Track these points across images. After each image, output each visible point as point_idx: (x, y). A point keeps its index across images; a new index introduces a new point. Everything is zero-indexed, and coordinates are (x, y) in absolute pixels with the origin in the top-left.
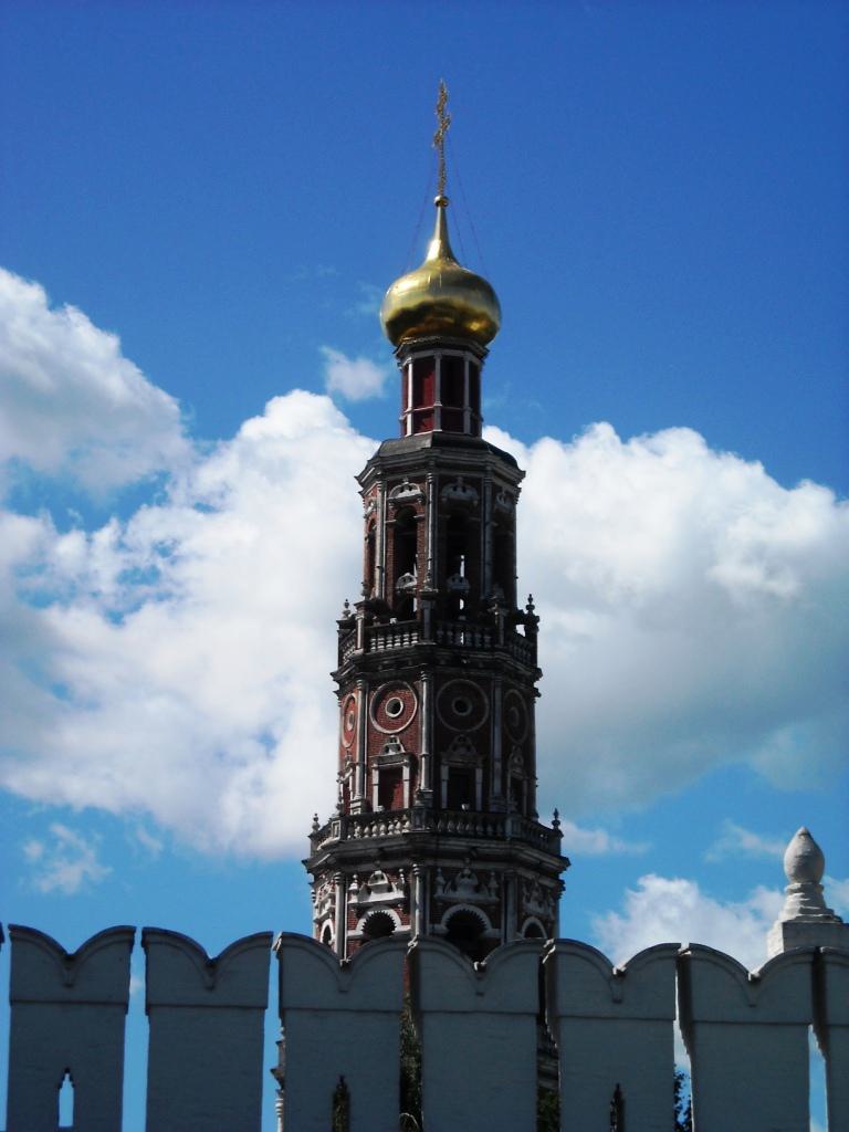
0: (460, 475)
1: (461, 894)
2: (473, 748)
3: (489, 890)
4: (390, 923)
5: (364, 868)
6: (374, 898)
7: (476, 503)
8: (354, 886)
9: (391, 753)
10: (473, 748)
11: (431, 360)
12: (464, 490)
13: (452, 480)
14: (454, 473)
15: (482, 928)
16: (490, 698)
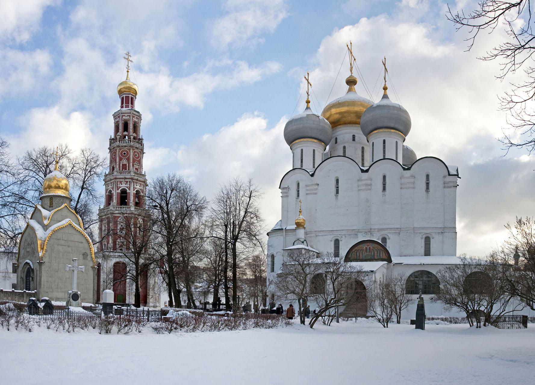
6: (122, 185)
8: (119, 183)
9: (124, 161)
11: (129, 96)
13: (135, 117)
14: (135, 116)
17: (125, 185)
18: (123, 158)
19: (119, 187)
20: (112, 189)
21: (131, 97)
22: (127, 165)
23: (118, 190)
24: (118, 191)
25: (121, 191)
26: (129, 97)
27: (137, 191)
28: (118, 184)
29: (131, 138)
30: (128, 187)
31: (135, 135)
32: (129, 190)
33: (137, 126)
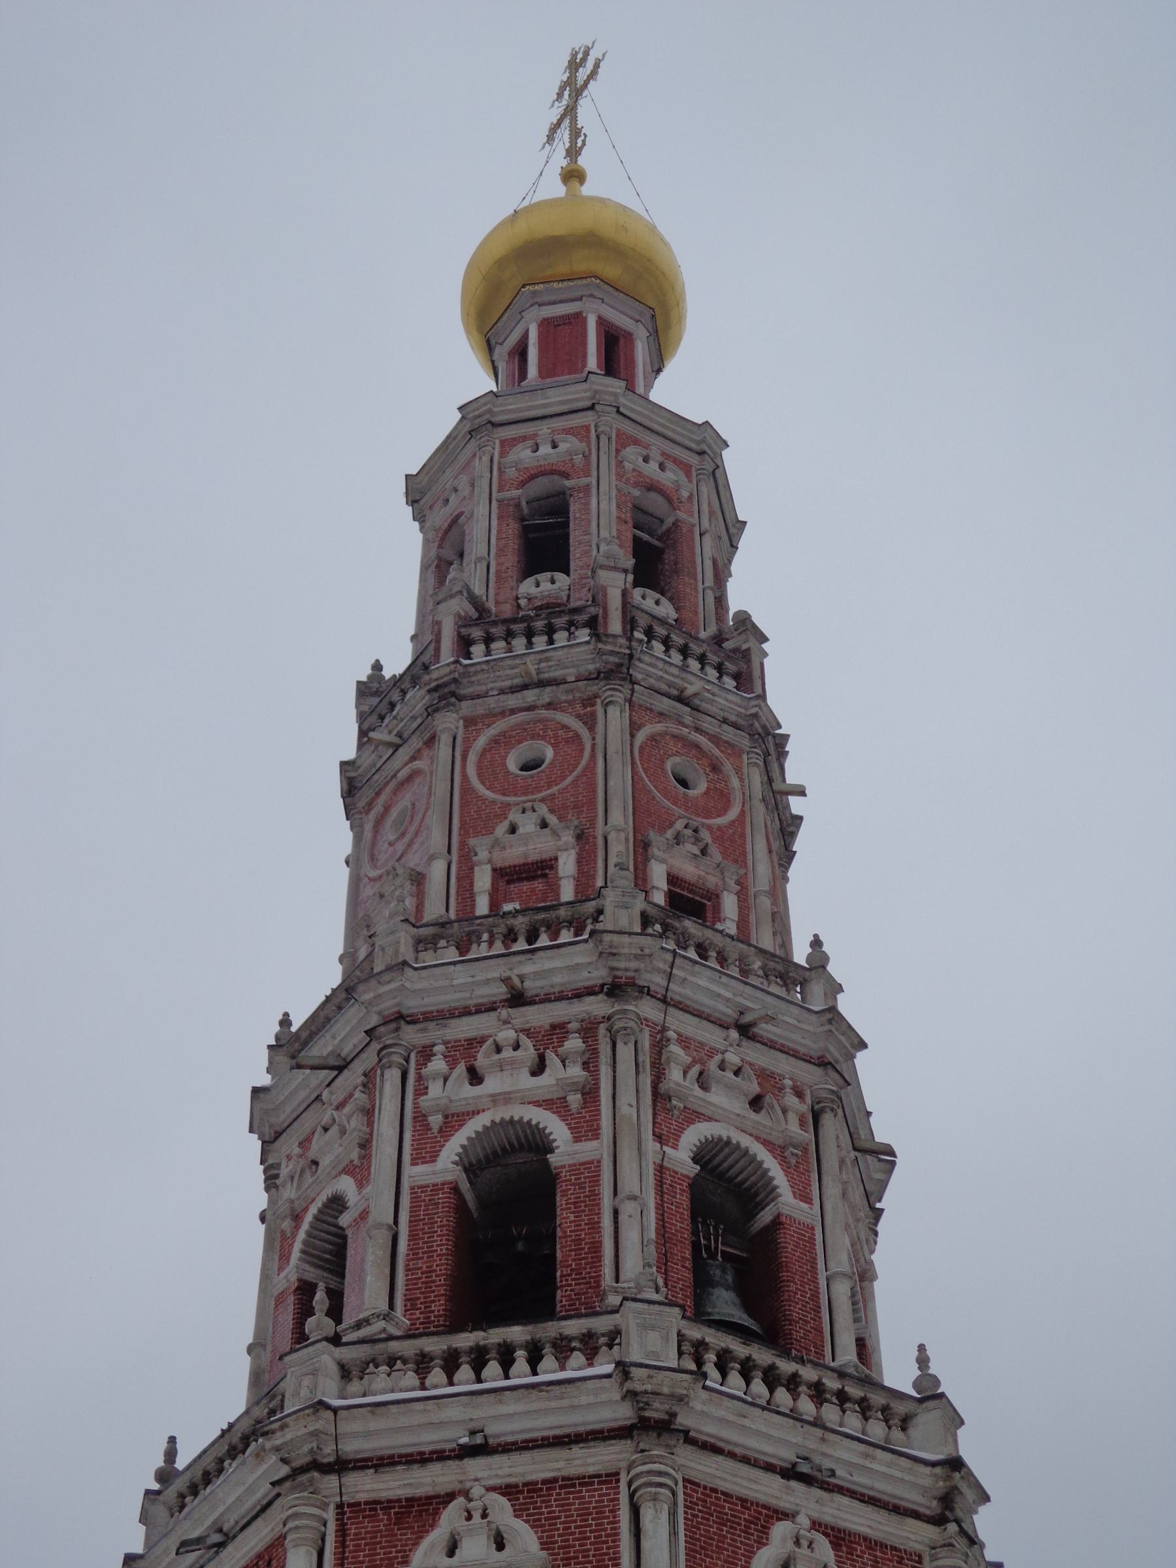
1: (717, 1098)
2: (714, 850)
3: (785, 1111)
6: (492, 1084)
8: (438, 1064)
10: (714, 850)
11: (577, 320)
12: (662, 467)
15: (771, 1192)
16: (741, 780)
17: (526, 1082)
18: (507, 807)
19: (436, 1120)
21: (601, 322)
22: (567, 865)
23: (427, 1153)
24: (420, 1169)
26: (584, 321)
27: (706, 1155)
28: (422, 1091)
29: (604, 590)
31: (666, 610)
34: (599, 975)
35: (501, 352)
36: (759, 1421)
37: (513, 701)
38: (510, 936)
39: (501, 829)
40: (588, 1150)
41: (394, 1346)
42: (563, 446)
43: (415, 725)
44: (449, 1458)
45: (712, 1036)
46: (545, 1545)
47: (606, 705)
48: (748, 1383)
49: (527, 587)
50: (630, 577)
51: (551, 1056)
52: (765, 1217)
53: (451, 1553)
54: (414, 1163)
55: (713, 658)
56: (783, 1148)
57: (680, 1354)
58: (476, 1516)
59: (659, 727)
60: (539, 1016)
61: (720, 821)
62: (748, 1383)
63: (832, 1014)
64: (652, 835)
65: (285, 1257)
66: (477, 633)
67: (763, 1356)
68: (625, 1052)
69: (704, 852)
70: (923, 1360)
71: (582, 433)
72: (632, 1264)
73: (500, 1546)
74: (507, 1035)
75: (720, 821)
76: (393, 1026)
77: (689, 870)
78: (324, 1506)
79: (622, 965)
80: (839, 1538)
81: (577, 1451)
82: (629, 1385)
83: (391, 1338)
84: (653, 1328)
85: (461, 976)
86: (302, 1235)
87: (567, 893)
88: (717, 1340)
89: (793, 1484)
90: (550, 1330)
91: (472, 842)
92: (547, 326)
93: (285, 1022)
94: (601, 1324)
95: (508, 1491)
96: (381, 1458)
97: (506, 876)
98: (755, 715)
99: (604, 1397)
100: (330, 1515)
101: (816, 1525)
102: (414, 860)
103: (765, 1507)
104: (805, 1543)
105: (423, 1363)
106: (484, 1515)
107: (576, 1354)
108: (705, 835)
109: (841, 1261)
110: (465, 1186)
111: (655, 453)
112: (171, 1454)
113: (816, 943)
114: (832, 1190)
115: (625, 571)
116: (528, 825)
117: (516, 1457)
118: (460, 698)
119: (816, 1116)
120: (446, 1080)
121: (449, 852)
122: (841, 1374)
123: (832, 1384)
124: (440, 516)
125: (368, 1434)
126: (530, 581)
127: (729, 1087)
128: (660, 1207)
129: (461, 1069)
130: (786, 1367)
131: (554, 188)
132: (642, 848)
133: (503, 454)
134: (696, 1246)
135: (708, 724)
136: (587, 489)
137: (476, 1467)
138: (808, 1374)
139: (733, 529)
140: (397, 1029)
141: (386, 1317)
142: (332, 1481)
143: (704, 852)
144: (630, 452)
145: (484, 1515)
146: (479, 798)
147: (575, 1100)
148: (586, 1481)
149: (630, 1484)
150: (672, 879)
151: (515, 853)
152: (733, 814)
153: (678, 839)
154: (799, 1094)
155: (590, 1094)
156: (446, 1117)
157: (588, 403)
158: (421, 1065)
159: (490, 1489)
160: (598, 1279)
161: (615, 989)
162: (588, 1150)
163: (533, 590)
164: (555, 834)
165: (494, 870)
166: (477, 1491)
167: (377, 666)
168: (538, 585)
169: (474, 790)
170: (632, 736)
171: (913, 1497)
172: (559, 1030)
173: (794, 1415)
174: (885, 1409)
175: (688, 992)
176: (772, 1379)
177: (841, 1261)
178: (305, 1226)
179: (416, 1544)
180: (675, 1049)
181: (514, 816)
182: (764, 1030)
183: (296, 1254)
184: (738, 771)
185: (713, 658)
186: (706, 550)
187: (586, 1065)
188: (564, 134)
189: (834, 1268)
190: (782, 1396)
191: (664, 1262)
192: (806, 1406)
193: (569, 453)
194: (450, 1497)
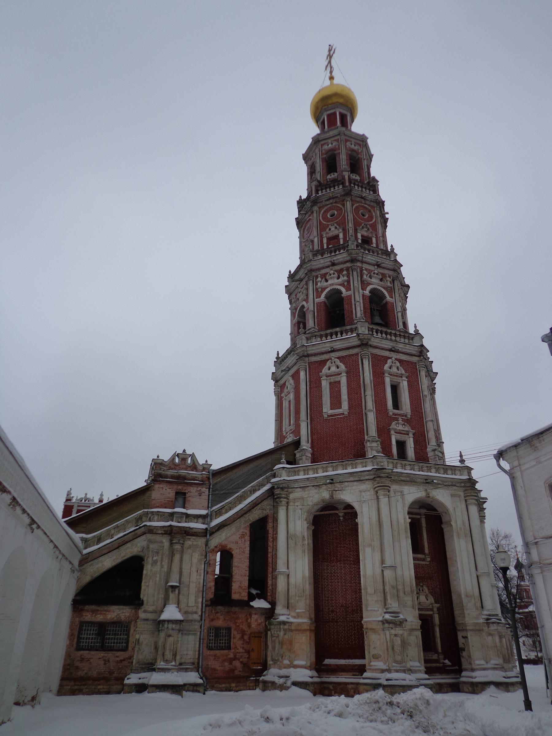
0: (353, 141)
1: (373, 280)
3: (387, 281)
4: (340, 292)
5: (323, 271)
6: (330, 282)
7: (360, 151)
8: (319, 279)
11: (335, 113)
12: (355, 145)
15: (385, 297)
16: (375, 213)
17: (336, 281)
18: (328, 225)
19: (320, 290)
20: (304, 303)
21: (340, 113)
22: (341, 236)
23: (319, 296)
25: (327, 297)
27: (371, 291)
28: (316, 284)
30: (346, 283)
31: (358, 178)
32: (348, 289)
33: (359, 158)
34: (349, 258)
35: (320, 123)
36: (384, 342)
37: (328, 203)
38: (331, 252)
39: (328, 230)
40: (349, 293)
41: (315, 334)
42: (334, 144)
43: (309, 209)
44: (327, 353)
45: (372, 268)
46: (346, 367)
47: (346, 201)
48: (382, 335)
49: (329, 177)
50: (349, 173)
51: (341, 275)
52: (384, 302)
53: (329, 370)
54: (316, 298)
55: (368, 188)
56: (387, 288)
57: (368, 330)
58: (333, 363)
59: (358, 204)
60: (337, 268)
61: (371, 222)
62: (382, 335)
63: (396, 260)
64: (357, 228)
65: (295, 317)
66: (319, 188)
67: (384, 329)
68: (355, 273)
69: (368, 229)
70: (415, 327)
71: (337, 140)
72: (359, 314)
73: (338, 368)
74: (332, 272)
75: (371, 222)
76: (310, 272)
77: (365, 234)
78: (306, 363)
79: (353, 256)
80: (400, 361)
81: (351, 350)
82: (359, 338)
83: (316, 332)
84: (363, 327)
85: (322, 261)
86: (297, 313)
87: (342, 242)
88: (375, 327)
89: (391, 352)
90: (344, 328)
91: (322, 233)
92: (329, 116)
93: (290, 272)
94: (353, 326)
95: (339, 358)
96: (315, 354)
97: (329, 239)
98: (377, 199)
99: (355, 340)
100: (307, 364)
101: (396, 359)
102: (311, 238)
103: (386, 357)
104: (394, 363)
105: (321, 336)
106: (335, 363)
107: (349, 332)
108: (368, 226)
109: (399, 309)
110: (326, 302)
111: (353, 143)
112: (278, 354)
113: (392, 246)
114: (397, 295)
115: (348, 171)
116: (333, 229)
117: (340, 352)
118: (317, 203)
119: (393, 281)
120: (321, 282)
121: (318, 235)
122: (400, 331)
123: (398, 333)
124: (310, 163)
125: (313, 350)
126: (329, 175)
127: (376, 278)
128: (363, 303)
129: (324, 279)
130: (389, 331)
131: (328, 82)
132: (356, 231)
133: (322, 147)
134: (371, 309)
135: (368, 202)
136: (339, 153)
137: (333, 355)
138: (393, 332)
139: (370, 157)
140: (311, 273)
141: (314, 328)
142: (307, 359)
143: (368, 229)
144: (348, 143)
145: (335, 363)
146: (323, 223)
147: (346, 283)
148: (352, 355)
149: (361, 355)
150: (362, 236)
151: (331, 234)
152: (374, 221)
153: (363, 228)
154: (390, 277)
155: (349, 282)
156: (322, 289)
157: (338, 134)
158: (316, 279)
159: (335, 358)
160: (353, 317)
161: (353, 261)
162: (349, 293)
163: (330, 177)
164: (338, 230)
165: (327, 238)
166: (333, 358)
167: (301, 197)
168: (331, 176)
169: (321, 222)
170: (352, 207)
171: (414, 352)
172: (341, 270)
173: (391, 340)
174: (408, 337)
175: (366, 260)
176: (386, 333)
177: (399, 309)
178: (298, 311)
179: (323, 368)
180: (365, 272)
181: (330, 227)
182: (383, 265)
183: (296, 316)
184: (374, 211)
185: (368, 188)
186: (365, 163)
187: (347, 277)
188: (329, 68)
189: (398, 310)
190: (389, 337)
191: (365, 312)
192: (393, 338)
193: (335, 146)
194: (328, 360)
